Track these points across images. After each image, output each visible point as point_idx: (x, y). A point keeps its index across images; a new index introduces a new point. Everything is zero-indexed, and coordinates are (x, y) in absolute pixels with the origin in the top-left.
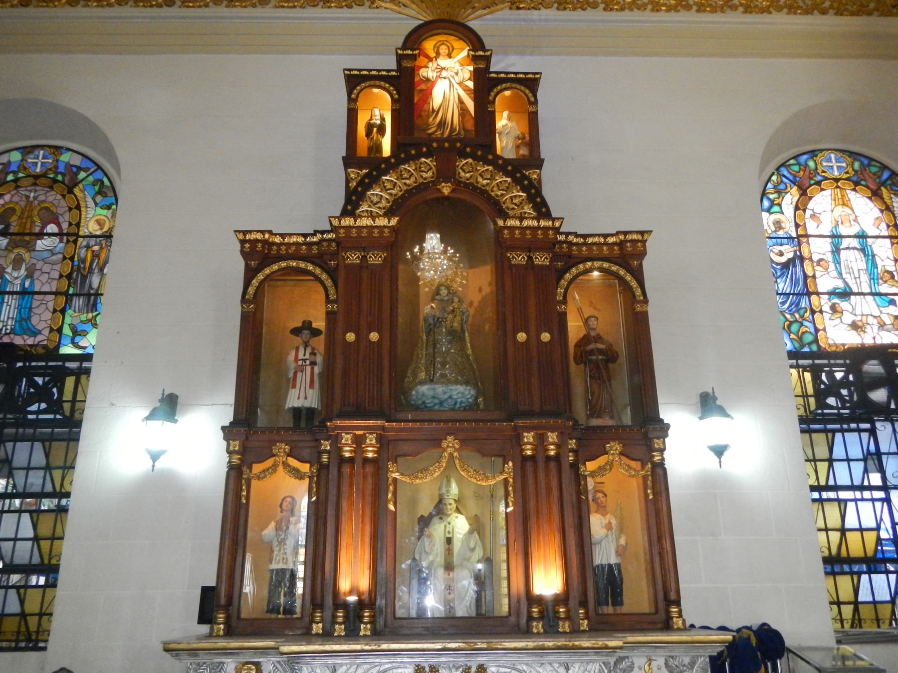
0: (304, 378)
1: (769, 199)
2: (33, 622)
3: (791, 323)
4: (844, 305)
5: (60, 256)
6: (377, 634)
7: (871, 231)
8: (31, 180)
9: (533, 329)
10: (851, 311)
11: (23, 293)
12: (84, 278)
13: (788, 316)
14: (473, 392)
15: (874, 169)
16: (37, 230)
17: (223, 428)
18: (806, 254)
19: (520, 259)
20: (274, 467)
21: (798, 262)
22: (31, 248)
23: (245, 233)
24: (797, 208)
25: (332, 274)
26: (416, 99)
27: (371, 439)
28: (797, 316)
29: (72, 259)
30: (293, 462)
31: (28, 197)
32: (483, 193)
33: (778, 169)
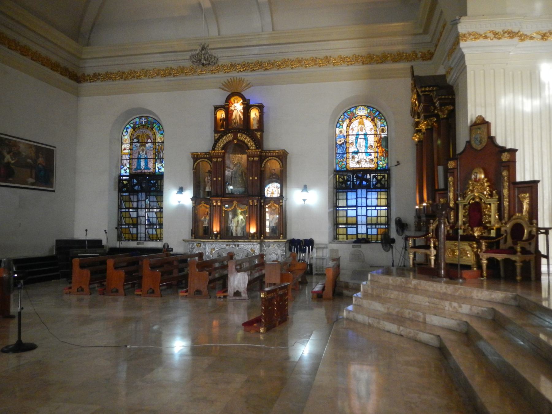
0: (209, 184)
1: (339, 124)
2: (159, 236)
3: (340, 162)
4: (356, 156)
5: (152, 148)
6: (221, 239)
7: (369, 132)
8: (142, 127)
9: (254, 176)
10: (358, 157)
11: (146, 159)
12: (159, 154)
13: (339, 160)
14: (244, 189)
15: (374, 112)
16: (146, 141)
17: (191, 198)
18: (347, 141)
19: (251, 159)
20: (201, 206)
21: (345, 144)
22: (145, 146)
23: (192, 153)
24: (347, 126)
25: (211, 161)
26: (229, 116)
27: (219, 202)
28: (342, 160)
29: (155, 149)
30: (205, 205)
31: (142, 132)
32: (244, 142)
33: (343, 114)
